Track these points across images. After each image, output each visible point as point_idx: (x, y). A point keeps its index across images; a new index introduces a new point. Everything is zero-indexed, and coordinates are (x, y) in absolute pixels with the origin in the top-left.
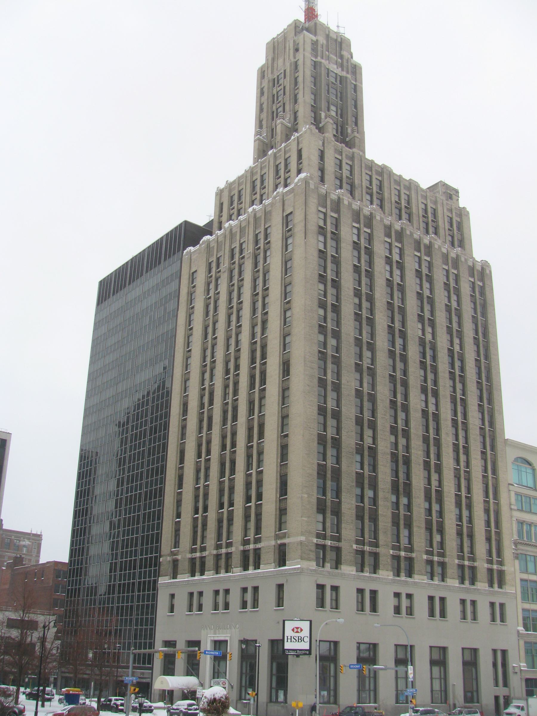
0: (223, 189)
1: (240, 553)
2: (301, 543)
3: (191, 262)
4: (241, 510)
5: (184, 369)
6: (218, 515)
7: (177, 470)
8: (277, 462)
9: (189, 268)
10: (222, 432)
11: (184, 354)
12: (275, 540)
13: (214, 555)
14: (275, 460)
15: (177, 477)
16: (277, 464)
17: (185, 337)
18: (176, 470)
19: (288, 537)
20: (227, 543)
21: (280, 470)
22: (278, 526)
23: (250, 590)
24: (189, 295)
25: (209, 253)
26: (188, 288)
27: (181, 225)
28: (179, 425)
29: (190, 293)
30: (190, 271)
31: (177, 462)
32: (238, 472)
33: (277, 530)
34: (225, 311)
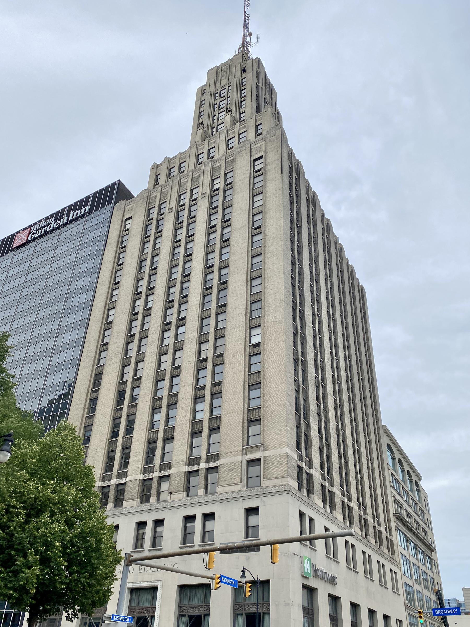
0: (160, 165)
1: (183, 474)
2: (287, 455)
3: (124, 211)
4: (188, 425)
5: (109, 299)
6: (148, 435)
7: (89, 393)
8: (245, 371)
9: (122, 215)
10: (160, 350)
11: (109, 286)
12: (242, 455)
13: (140, 479)
14: (242, 369)
15: (88, 400)
16: (244, 374)
17: (112, 272)
18: (87, 394)
19: (265, 450)
20: (161, 465)
21: (249, 379)
22: (246, 439)
23: (199, 519)
24: (121, 237)
25: (149, 201)
26: (120, 231)
27: (113, 185)
28: (97, 349)
29: (121, 235)
30: (123, 218)
31: (89, 385)
32: (184, 386)
33: (245, 444)
34: (170, 244)
